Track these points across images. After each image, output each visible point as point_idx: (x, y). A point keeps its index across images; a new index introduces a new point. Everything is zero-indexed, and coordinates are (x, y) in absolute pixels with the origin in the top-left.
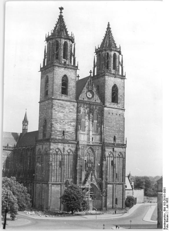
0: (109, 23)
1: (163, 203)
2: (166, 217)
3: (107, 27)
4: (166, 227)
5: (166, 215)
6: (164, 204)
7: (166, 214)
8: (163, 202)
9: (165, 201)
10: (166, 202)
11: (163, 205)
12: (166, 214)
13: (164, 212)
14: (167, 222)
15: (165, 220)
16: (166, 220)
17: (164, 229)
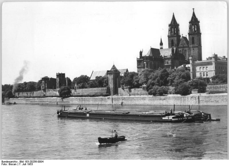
0: (173, 13)
1: (27, 160)
2: (14, 163)
3: (173, 15)
4: (4, 163)
5: (16, 163)
6: (27, 161)
7: (17, 163)
8: (29, 160)
9: (30, 162)
10: (29, 163)
11: (26, 160)
12: (17, 163)
13: (19, 161)
14: (9, 164)
15: (11, 162)
16: (11, 163)
17: (2, 161)
